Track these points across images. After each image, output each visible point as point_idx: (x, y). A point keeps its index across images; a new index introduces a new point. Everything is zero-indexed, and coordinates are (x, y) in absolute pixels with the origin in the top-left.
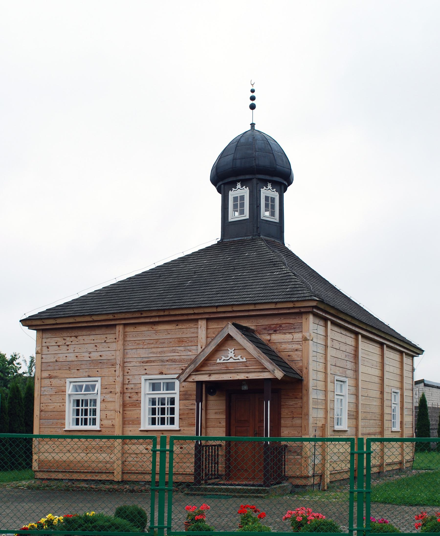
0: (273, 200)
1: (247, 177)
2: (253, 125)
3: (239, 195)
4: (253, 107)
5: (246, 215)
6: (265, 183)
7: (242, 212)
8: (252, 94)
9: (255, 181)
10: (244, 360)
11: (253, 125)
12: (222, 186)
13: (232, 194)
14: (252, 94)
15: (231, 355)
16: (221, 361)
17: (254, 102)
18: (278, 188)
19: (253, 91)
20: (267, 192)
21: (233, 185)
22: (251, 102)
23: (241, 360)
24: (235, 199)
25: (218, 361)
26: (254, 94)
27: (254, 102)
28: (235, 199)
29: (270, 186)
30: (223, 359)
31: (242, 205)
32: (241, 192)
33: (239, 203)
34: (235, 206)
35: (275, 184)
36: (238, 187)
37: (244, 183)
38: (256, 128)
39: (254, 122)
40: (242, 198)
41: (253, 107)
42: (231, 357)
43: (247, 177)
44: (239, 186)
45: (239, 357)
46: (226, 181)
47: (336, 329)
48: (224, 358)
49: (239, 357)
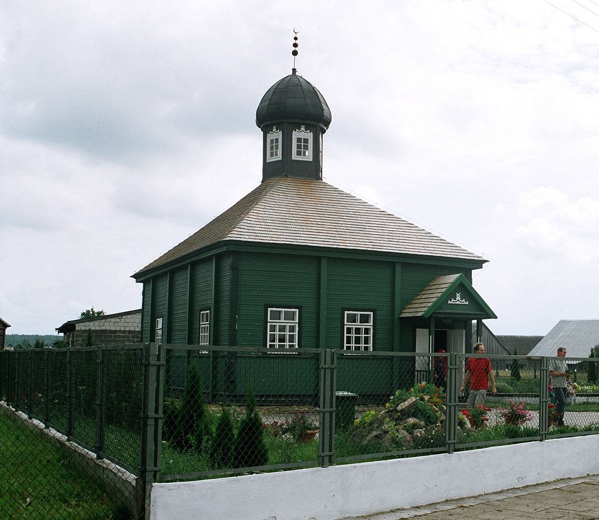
2: (294, 70)
3: (303, 137)
4: (295, 53)
5: (309, 156)
8: (294, 41)
10: (467, 303)
11: (294, 70)
12: (286, 124)
13: (296, 135)
14: (294, 41)
15: (458, 298)
16: (451, 302)
17: (296, 49)
19: (296, 39)
22: (294, 49)
23: (465, 303)
24: (299, 140)
25: (449, 302)
26: (297, 42)
27: (296, 49)
28: (299, 140)
36: (302, 129)
38: (297, 74)
39: (295, 68)
40: (306, 141)
41: (295, 53)
42: (458, 300)
44: (303, 129)
48: (453, 300)
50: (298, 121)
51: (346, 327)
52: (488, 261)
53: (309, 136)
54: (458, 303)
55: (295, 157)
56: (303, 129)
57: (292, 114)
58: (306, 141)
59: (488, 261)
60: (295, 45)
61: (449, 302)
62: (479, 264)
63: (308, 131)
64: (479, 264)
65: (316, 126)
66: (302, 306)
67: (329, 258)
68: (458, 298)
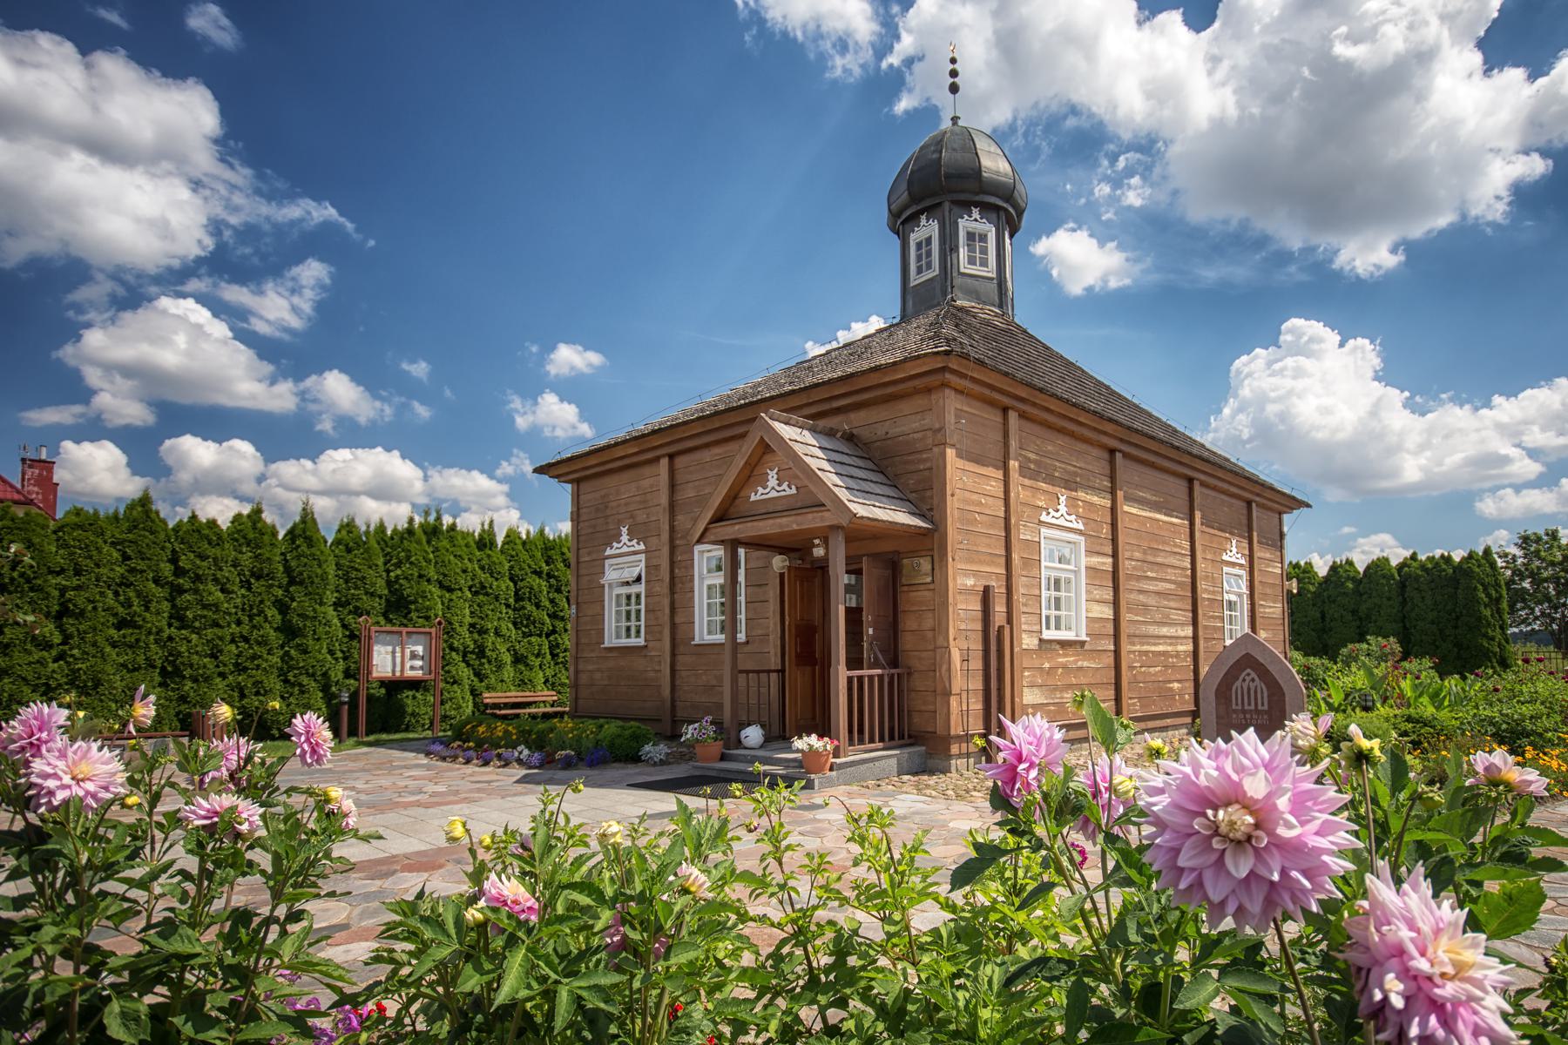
0: (983, 238)
5: (935, 271)
6: (966, 206)
7: (929, 266)
8: (951, 67)
9: (947, 205)
10: (794, 491)
13: (915, 237)
14: (951, 67)
15: (773, 482)
16: (758, 497)
18: (994, 216)
19: (953, 61)
21: (913, 219)
23: (789, 492)
24: (919, 246)
25: (753, 498)
29: (976, 213)
32: (928, 229)
35: (986, 208)
40: (929, 241)
41: (954, 89)
44: (923, 218)
45: (785, 486)
46: (904, 217)
47: (1128, 463)
48: (761, 490)
49: (785, 486)
50: (908, 213)
54: (774, 494)
55: (915, 280)
60: (954, 74)
61: (753, 498)
68: (773, 482)
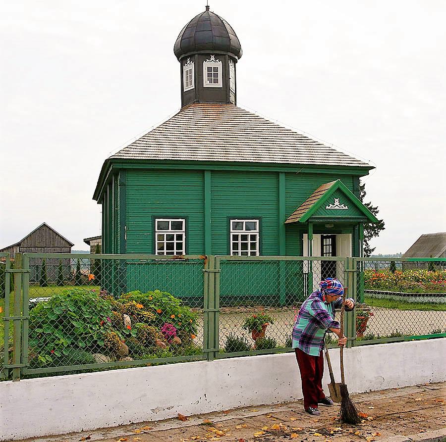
1: (222, 53)
2: (208, 7)
5: (220, 84)
7: (216, 81)
11: (208, 7)
12: (196, 55)
13: (206, 65)
15: (337, 203)
16: (329, 208)
20: (231, 65)
21: (208, 56)
23: (344, 208)
24: (209, 69)
25: (327, 207)
28: (209, 69)
30: (330, 206)
31: (216, 75)
33: (212, 72)
34: (209, 75)
37: (217, 56)
38: (210, 10)
40: (216, 69)
43: (222, 53)
44: (213, 58)
46: (202, 52)
48: (331, 205)
49: (343, 205)
51: (231, 234)
52: (375, 168)
53: (219, 65)
54: (337, 208)
55: (206, 84)
56: (213, 58)
57: (206, 45)
58: (216, 69)
59: (375, 168)
62: (365, 170)
63: (217, 61)
64: (365, 170)
65: (225, 55)
66: (187, 216)
67: (212, 171)
68: (337, 203)
